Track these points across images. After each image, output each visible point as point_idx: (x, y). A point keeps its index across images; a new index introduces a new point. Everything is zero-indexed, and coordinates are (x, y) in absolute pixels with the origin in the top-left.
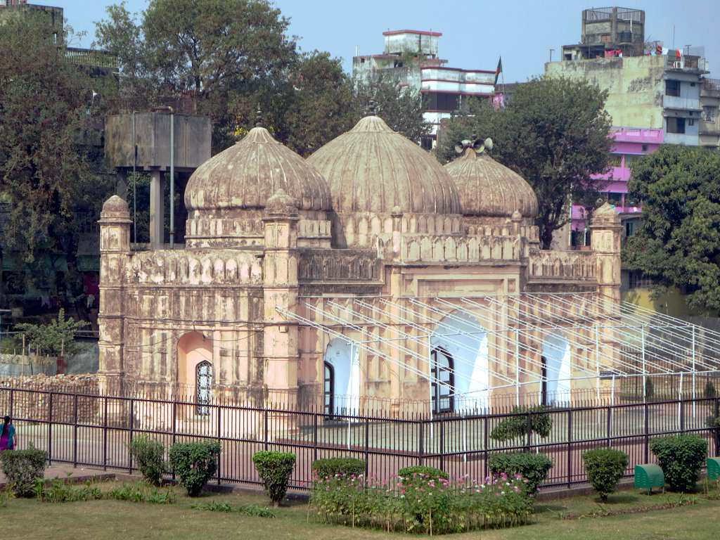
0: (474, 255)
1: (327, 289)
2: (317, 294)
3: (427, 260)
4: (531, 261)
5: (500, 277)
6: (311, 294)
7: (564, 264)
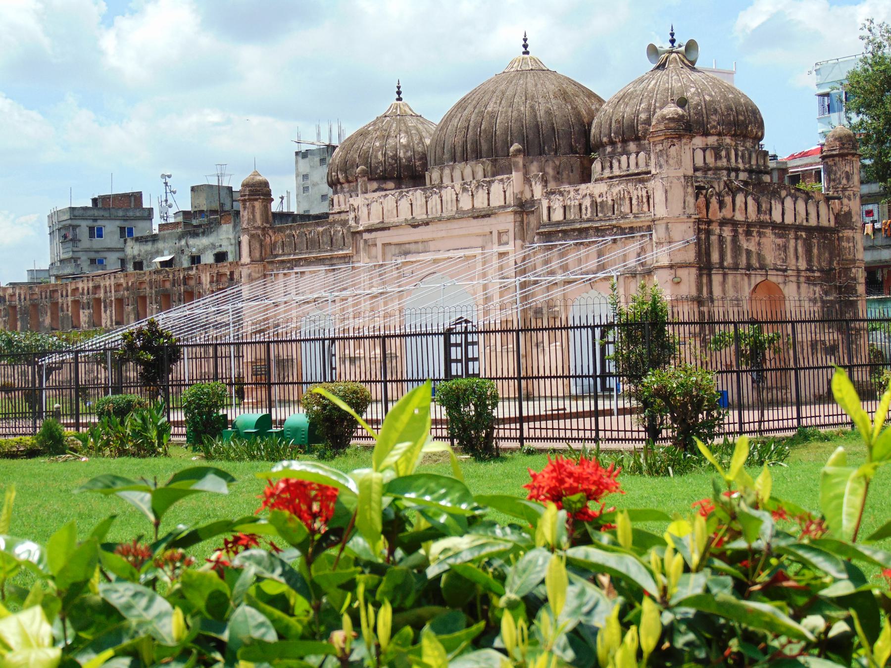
0: (450, 208)
1: (297, 263)
2: (289, 268)
3: (391, 220)
4: (545, 203)
5: (488, 230)
6: (284, 269)
7: (599, 200)
